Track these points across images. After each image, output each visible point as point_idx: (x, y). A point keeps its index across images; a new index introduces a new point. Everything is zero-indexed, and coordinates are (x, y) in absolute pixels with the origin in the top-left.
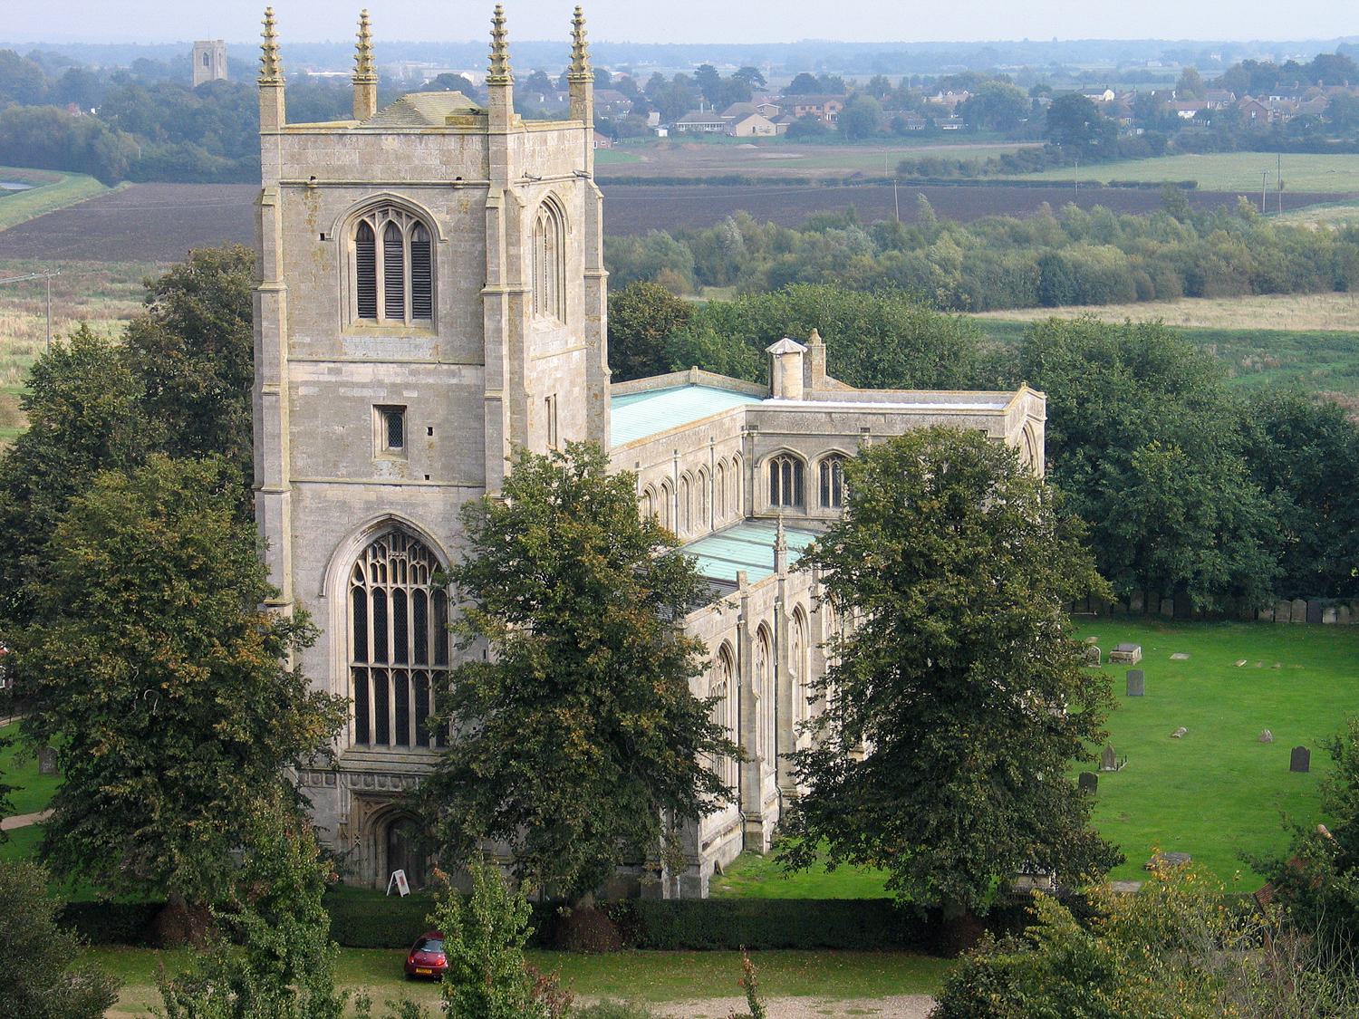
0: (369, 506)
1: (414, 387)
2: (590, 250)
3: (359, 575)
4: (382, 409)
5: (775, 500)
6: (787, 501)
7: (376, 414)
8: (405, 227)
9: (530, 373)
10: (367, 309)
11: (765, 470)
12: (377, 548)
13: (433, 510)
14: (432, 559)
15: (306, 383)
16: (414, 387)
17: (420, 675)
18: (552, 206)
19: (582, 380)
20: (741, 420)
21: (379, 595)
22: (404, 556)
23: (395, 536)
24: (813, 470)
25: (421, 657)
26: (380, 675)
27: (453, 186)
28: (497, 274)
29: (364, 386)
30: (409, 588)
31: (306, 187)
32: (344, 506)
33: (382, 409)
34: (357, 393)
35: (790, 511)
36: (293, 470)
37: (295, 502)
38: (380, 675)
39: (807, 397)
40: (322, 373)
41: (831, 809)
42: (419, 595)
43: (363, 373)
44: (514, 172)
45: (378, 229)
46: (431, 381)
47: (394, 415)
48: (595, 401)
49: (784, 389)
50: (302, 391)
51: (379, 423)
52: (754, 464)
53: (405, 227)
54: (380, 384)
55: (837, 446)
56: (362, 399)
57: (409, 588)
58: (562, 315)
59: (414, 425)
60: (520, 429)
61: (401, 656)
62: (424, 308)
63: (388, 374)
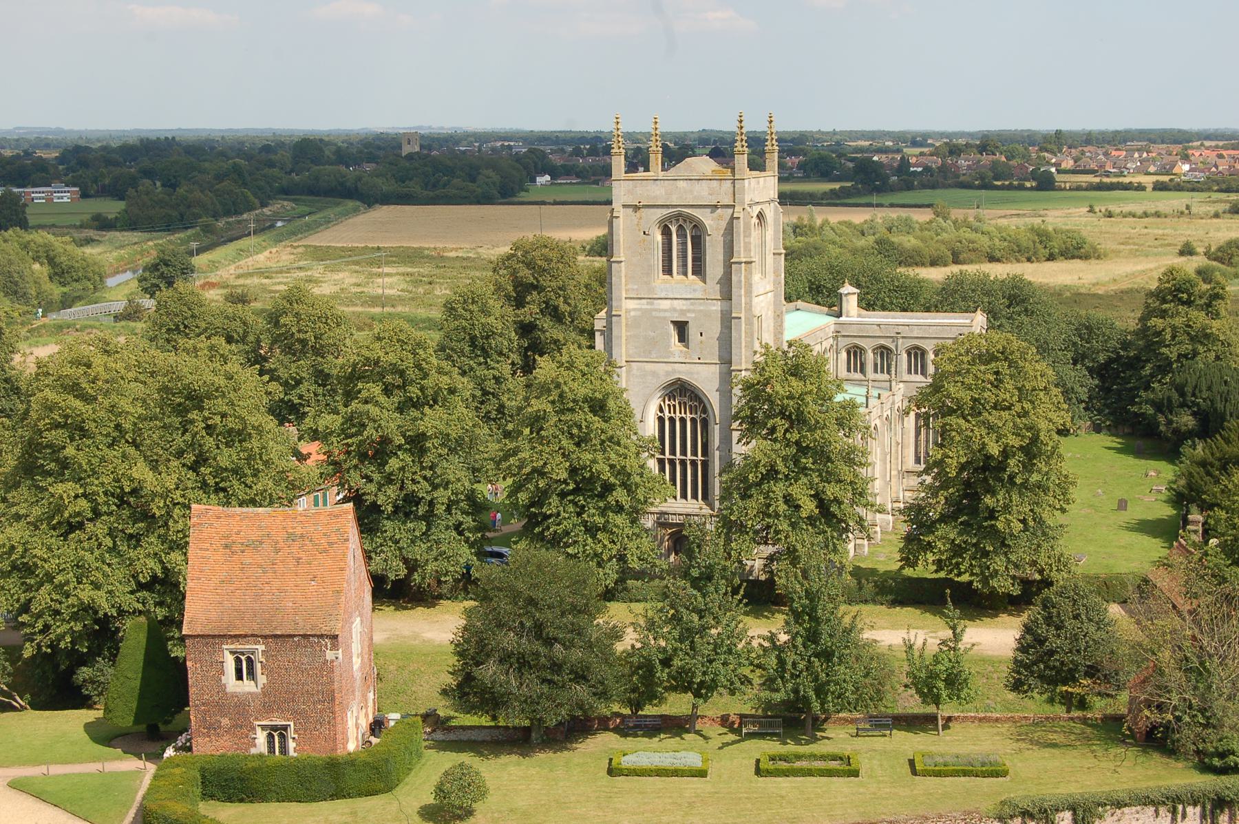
0: (668, 373)
1: (694, 311)
2: (776, 239)
3: (661, 410)
5: (849, 370)
6: (855, 371)
7: (672, 326)
9: (755, 300)
10: (668, 270)
11: (844, 355)
14: (701, 401)
15: (634, 310)
16: (694, 311)
18: (760, 216)
19: (772, 307)
20: (832, 328)
21: (672, 420)
22: (686, 399)
23: (681, 391)
27: (716, 206)
28: (739, 252)
29: (665, 311)
31: (636, 208)
32: (654, 374)
34: (662, 314)
35: (858, 376)
36: (628, 355)
37: (628, 372)
38: (672, 462)
39: (859, 316)
40: (643, 304)
41: (919, 526)
43: (665, 304)
44: (747, 201)
45: (674, 229)
47: (682, 328)
48: (779, 318)
49: (848, 312)
50: (632, 314)
54: (675, 310)
55: (882, 342)
56: (665, 318)
57: (688, 416)
58: (764, 273)
59: (693, 332)
62: (699, 270)
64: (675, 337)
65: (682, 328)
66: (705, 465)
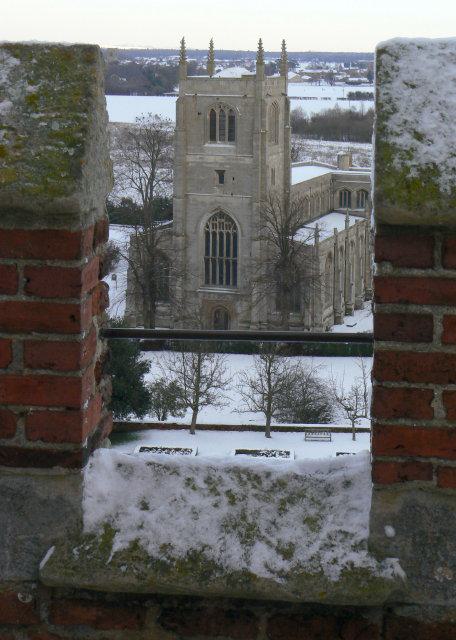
0: (212, 204)
1: (229, 164)
4: (217, 171)
8: (226, 112)
11: (338, 195)
12: (214, 218)
13: (236, 204)
14: (233, 222)
16: (229, 164)
17: (228, 262)
18: (275, 104)
21: (214, 234)
22: (223, 220)
23: (221, 215)
24: (354, 194)
25: (228, 255)
26: (214, 261)
30: (224, 231)
33: (217, 171)
34: (209, 165)
38: (214, 261)
42: (228, 235)
44: (264, 94)
45: (217, 111)
46: (234, 162)
47: (221, 174)
51: (217, 176)
52: (334, 192)
53: (226, 112)
56: (210, 168)
59: (227, 176)
60: (264, 179)
61: (221, 254)
63: (219, 159)
64: (217, 182)
65: (221, 174)
66: (235, 263)
